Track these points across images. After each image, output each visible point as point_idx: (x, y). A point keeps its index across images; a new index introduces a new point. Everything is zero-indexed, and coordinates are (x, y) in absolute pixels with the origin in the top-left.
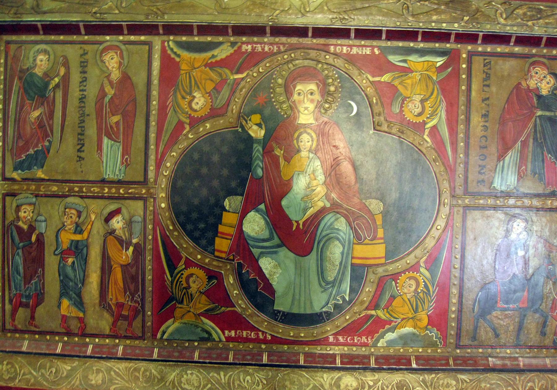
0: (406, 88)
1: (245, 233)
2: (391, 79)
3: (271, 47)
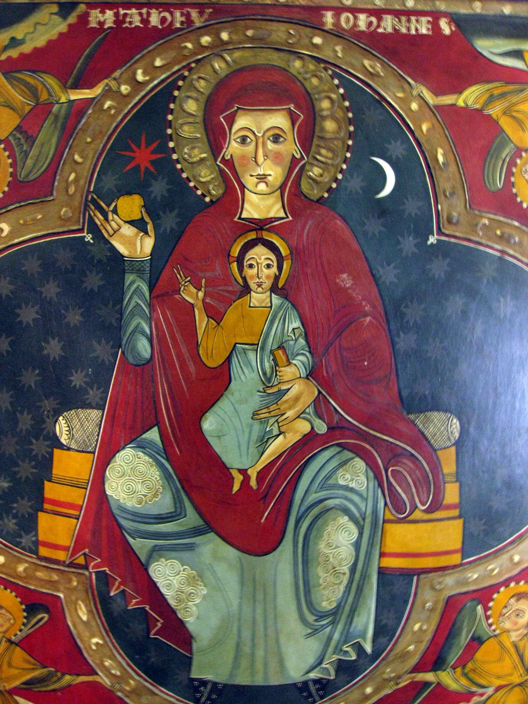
0: (520, 123)
1: (112, 502)
2: (482, 101)
3: (167, 15)
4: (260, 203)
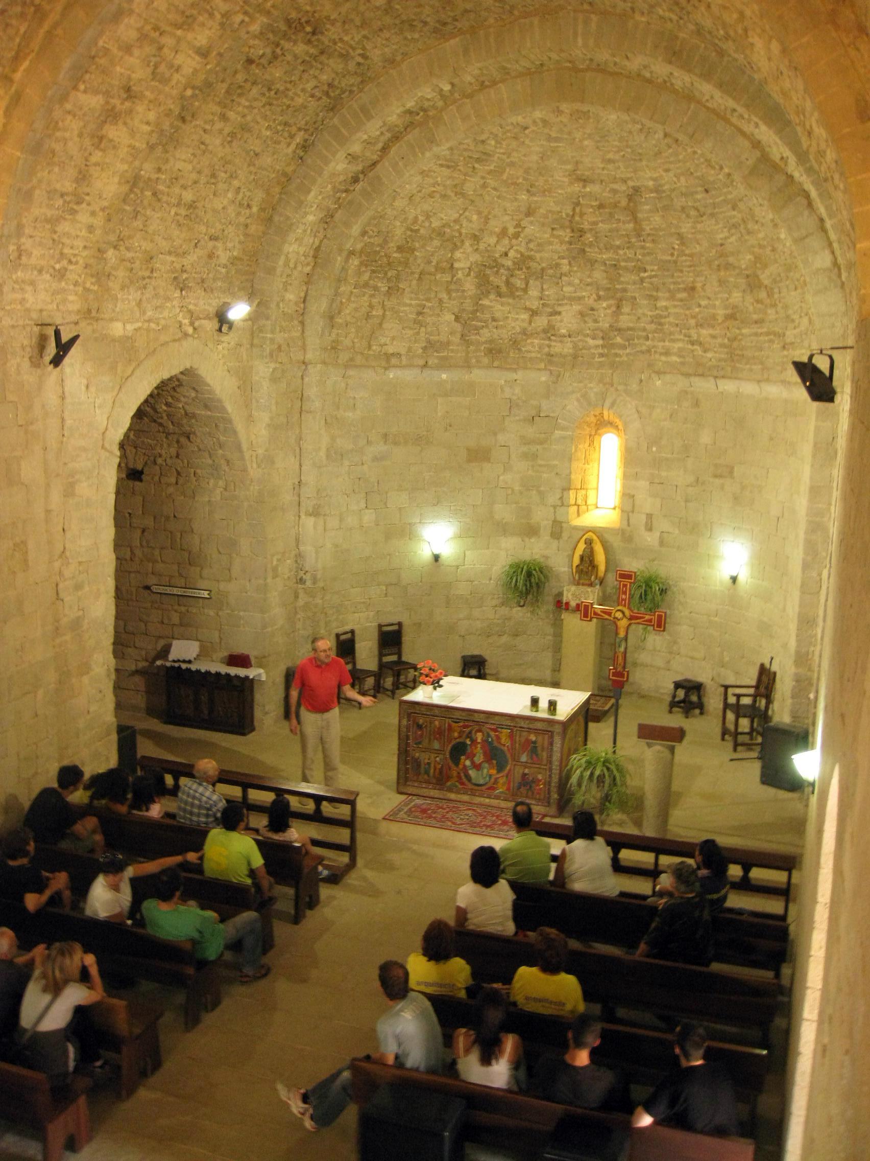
4: (479, 741)
